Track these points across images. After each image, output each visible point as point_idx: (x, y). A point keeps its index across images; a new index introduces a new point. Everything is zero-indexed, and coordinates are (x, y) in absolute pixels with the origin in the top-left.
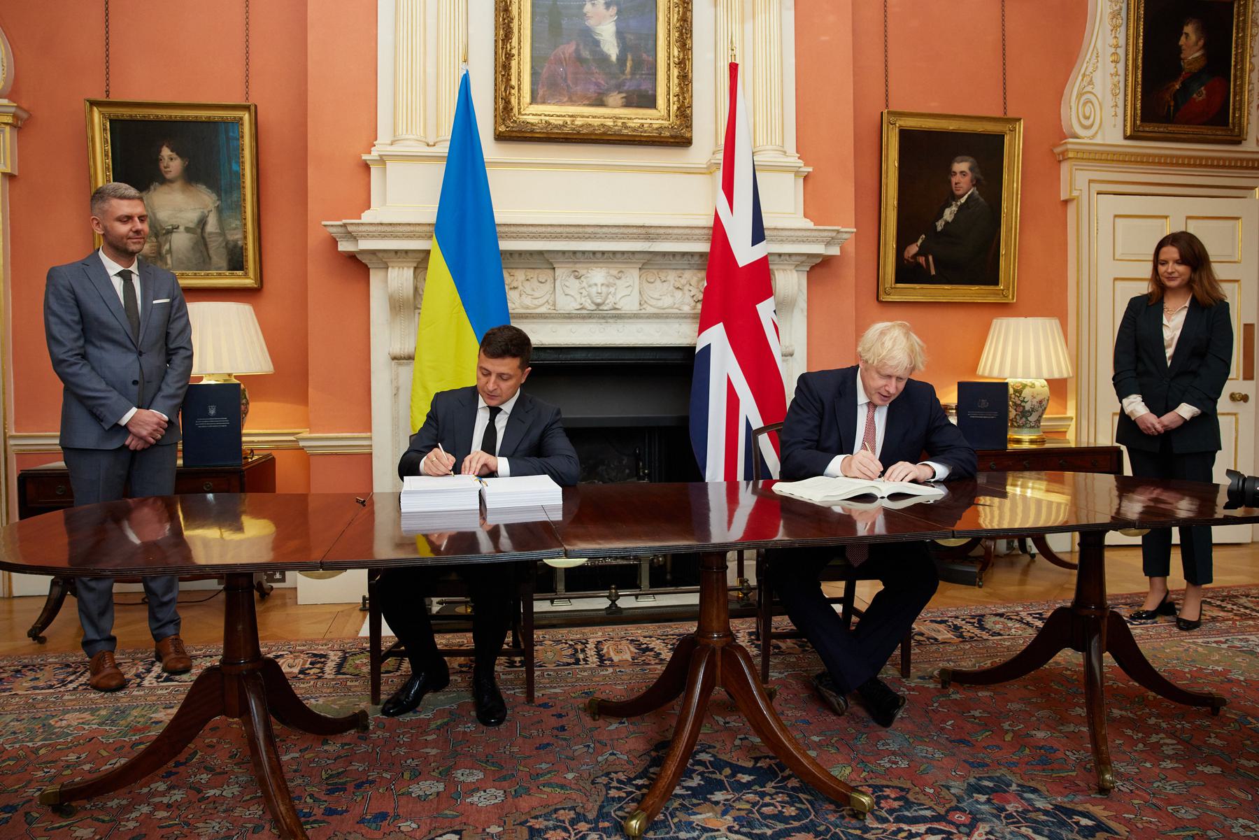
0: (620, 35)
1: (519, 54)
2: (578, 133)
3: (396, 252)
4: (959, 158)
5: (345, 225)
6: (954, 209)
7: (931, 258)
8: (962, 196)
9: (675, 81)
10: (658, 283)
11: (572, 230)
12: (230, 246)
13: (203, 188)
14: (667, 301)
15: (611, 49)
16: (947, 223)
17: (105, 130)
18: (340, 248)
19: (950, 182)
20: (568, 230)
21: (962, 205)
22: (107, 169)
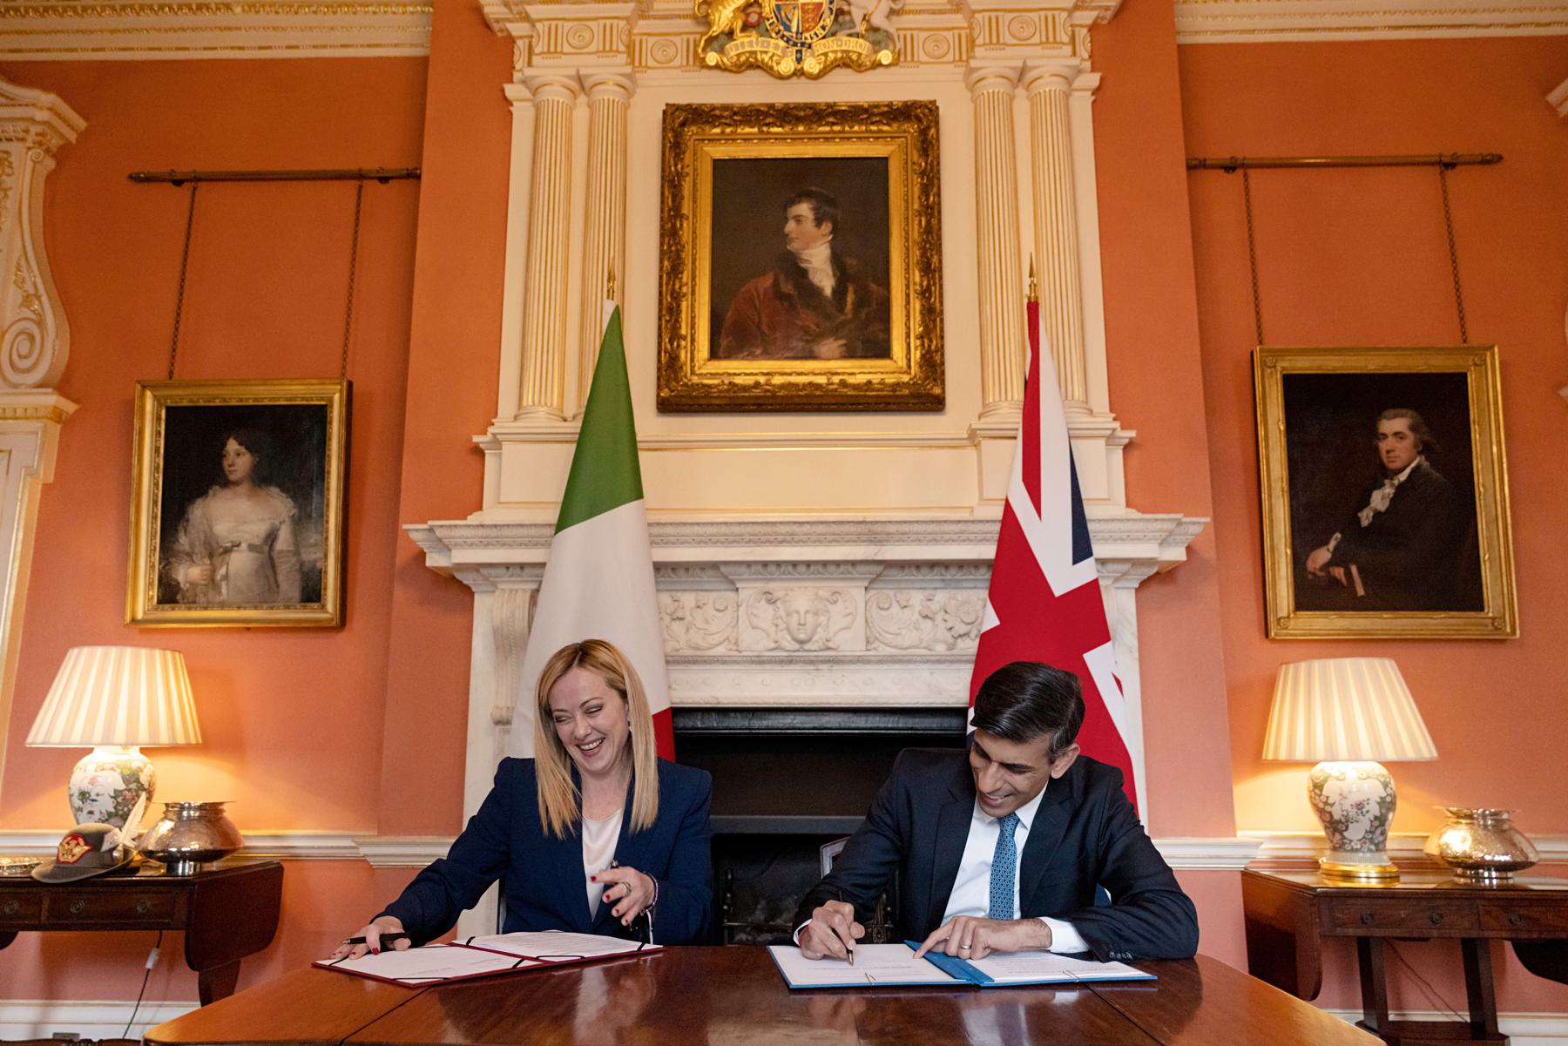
0: (836, 260)
1: (693, 293)
2: (774, 396)
3: (508, 566)
4: (1386, 413)
5: (431, 530)
6: (1388, 490)
7: (1354, 569)
8: (1402, 470)
9: (916, 317)
10: (895, 608)
11: (758, 529)
12: (305, 569)
13: (275, 490)
14: (910, 637)
15: (825, 281)
16: (1377, 514)
17: (159, 419)
19: (1376, 450)
20: (749, 529)
21: (1401, 485)
22: (157, 469)
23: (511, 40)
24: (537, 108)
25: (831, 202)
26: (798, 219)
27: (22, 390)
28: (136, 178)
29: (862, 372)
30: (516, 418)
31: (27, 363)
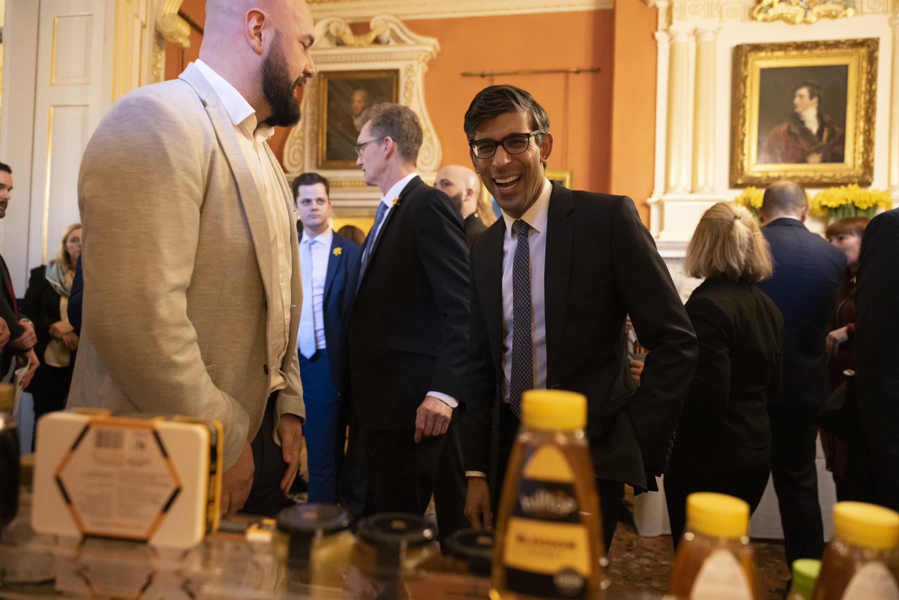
0: (820, 116)
15: (813, 125)
25: (818, 87)
26: (801, 96)
29: (830, 170)
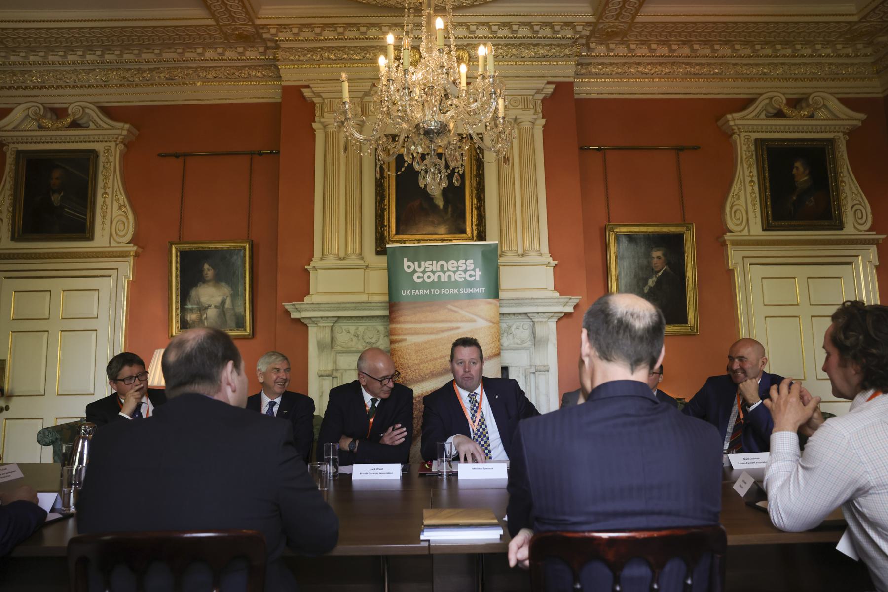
13: (223, 284)
18: (292, 317)
23: (313, 104)
24: (326, 133)
27: (122, 245)
28: (159, 155)
30: (321, 259)
31: (121, 233)
